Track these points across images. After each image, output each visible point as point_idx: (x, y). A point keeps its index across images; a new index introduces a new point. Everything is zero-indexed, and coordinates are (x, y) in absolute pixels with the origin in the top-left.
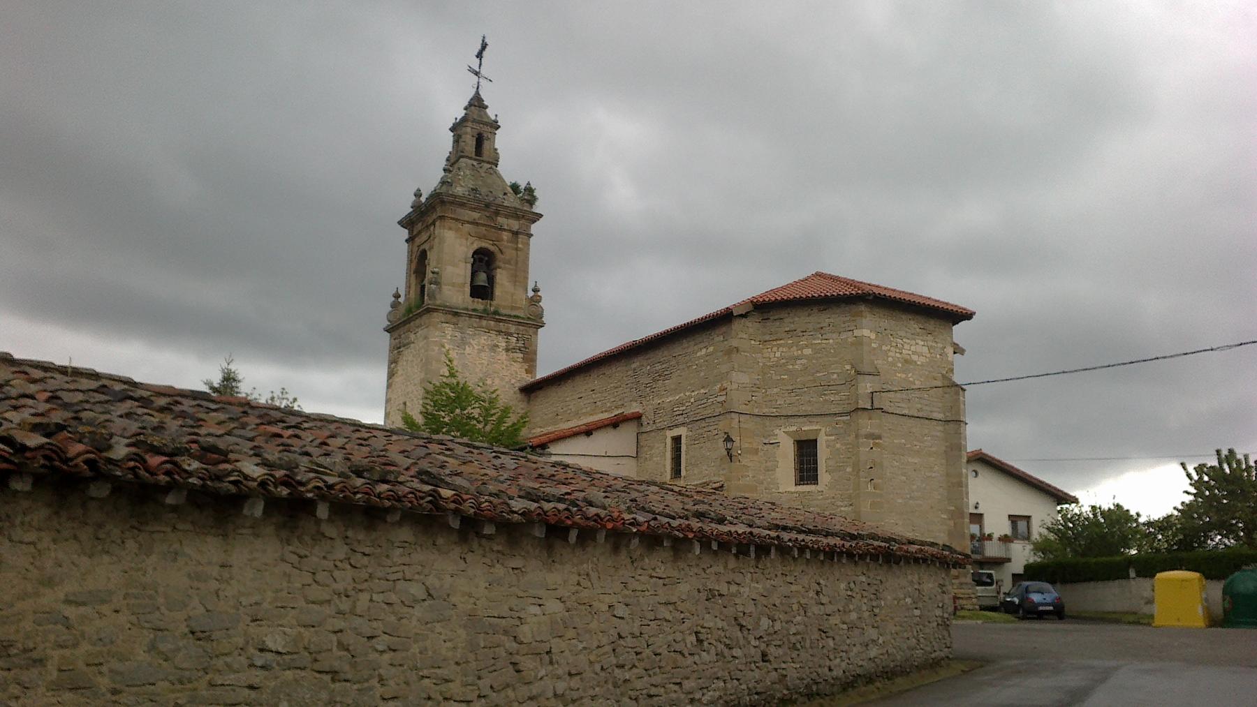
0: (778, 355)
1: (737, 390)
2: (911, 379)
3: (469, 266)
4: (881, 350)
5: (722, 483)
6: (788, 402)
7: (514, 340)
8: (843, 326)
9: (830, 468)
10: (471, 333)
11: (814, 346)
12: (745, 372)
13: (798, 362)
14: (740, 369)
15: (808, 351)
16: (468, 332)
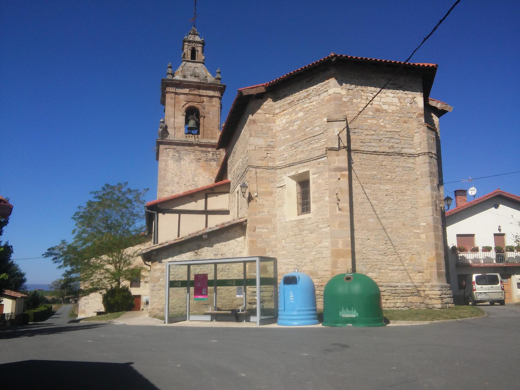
0: (284, 121)
1: (255, 150)
2: (382, 124)
3: (184, 117)
4: (352, 103)
5: (246, 218)
6: (290, 154)
7: (211, 155)
8: (321, 89)
9: (316, 199)
10: (184, 153)
11: (304, 110)
12: (260, 137)
13: (296, 123)
14: (257, 135)
15: (301, 114)
16: (183, 153)
